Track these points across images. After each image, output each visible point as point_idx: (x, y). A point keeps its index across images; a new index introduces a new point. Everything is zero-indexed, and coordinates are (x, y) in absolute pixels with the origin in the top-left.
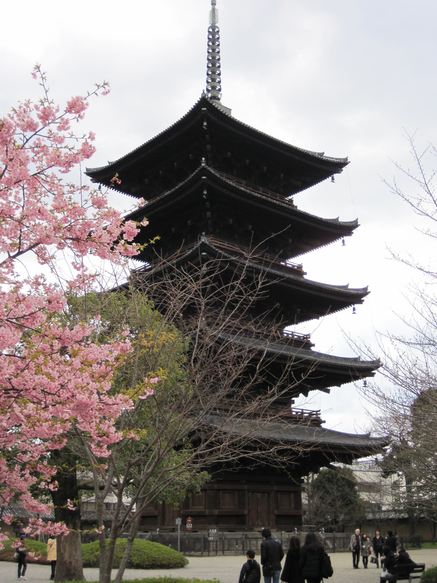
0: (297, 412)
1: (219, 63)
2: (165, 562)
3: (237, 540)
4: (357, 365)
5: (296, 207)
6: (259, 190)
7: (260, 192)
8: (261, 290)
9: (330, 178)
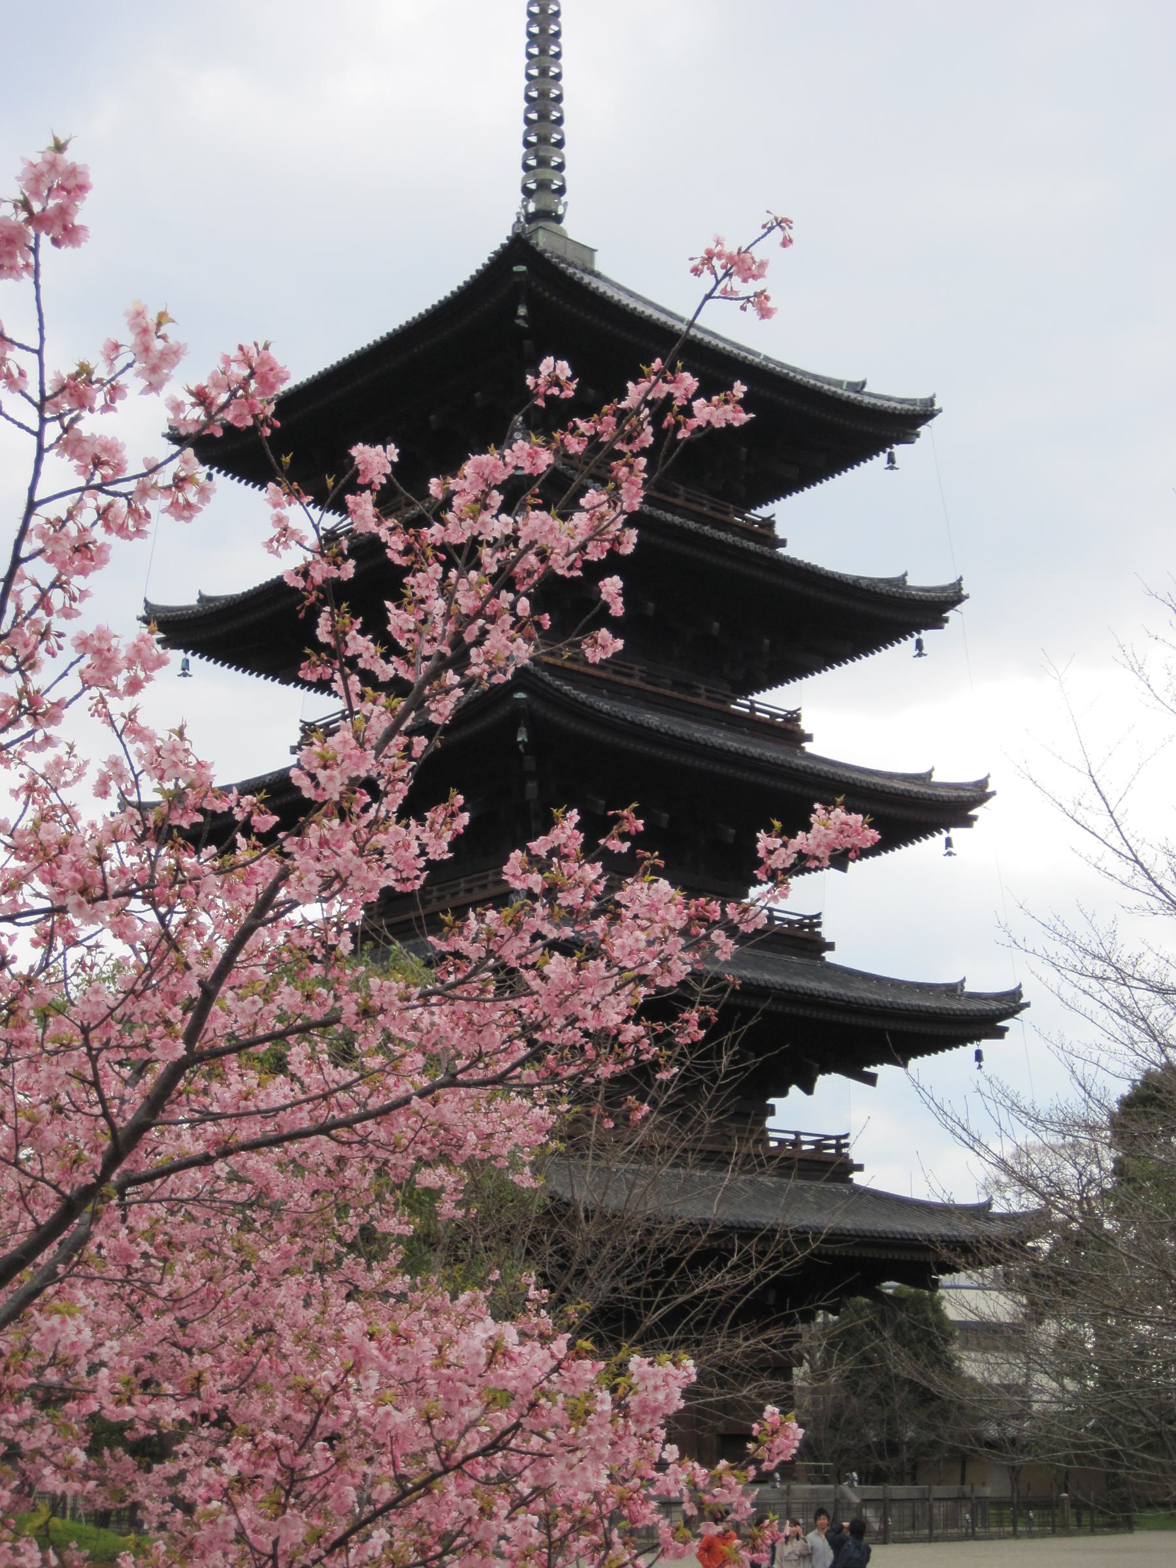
4: (955, 1005)
5: (783, 543)
6: (676, 496)
7: (679, 501)
9: (883, 457)
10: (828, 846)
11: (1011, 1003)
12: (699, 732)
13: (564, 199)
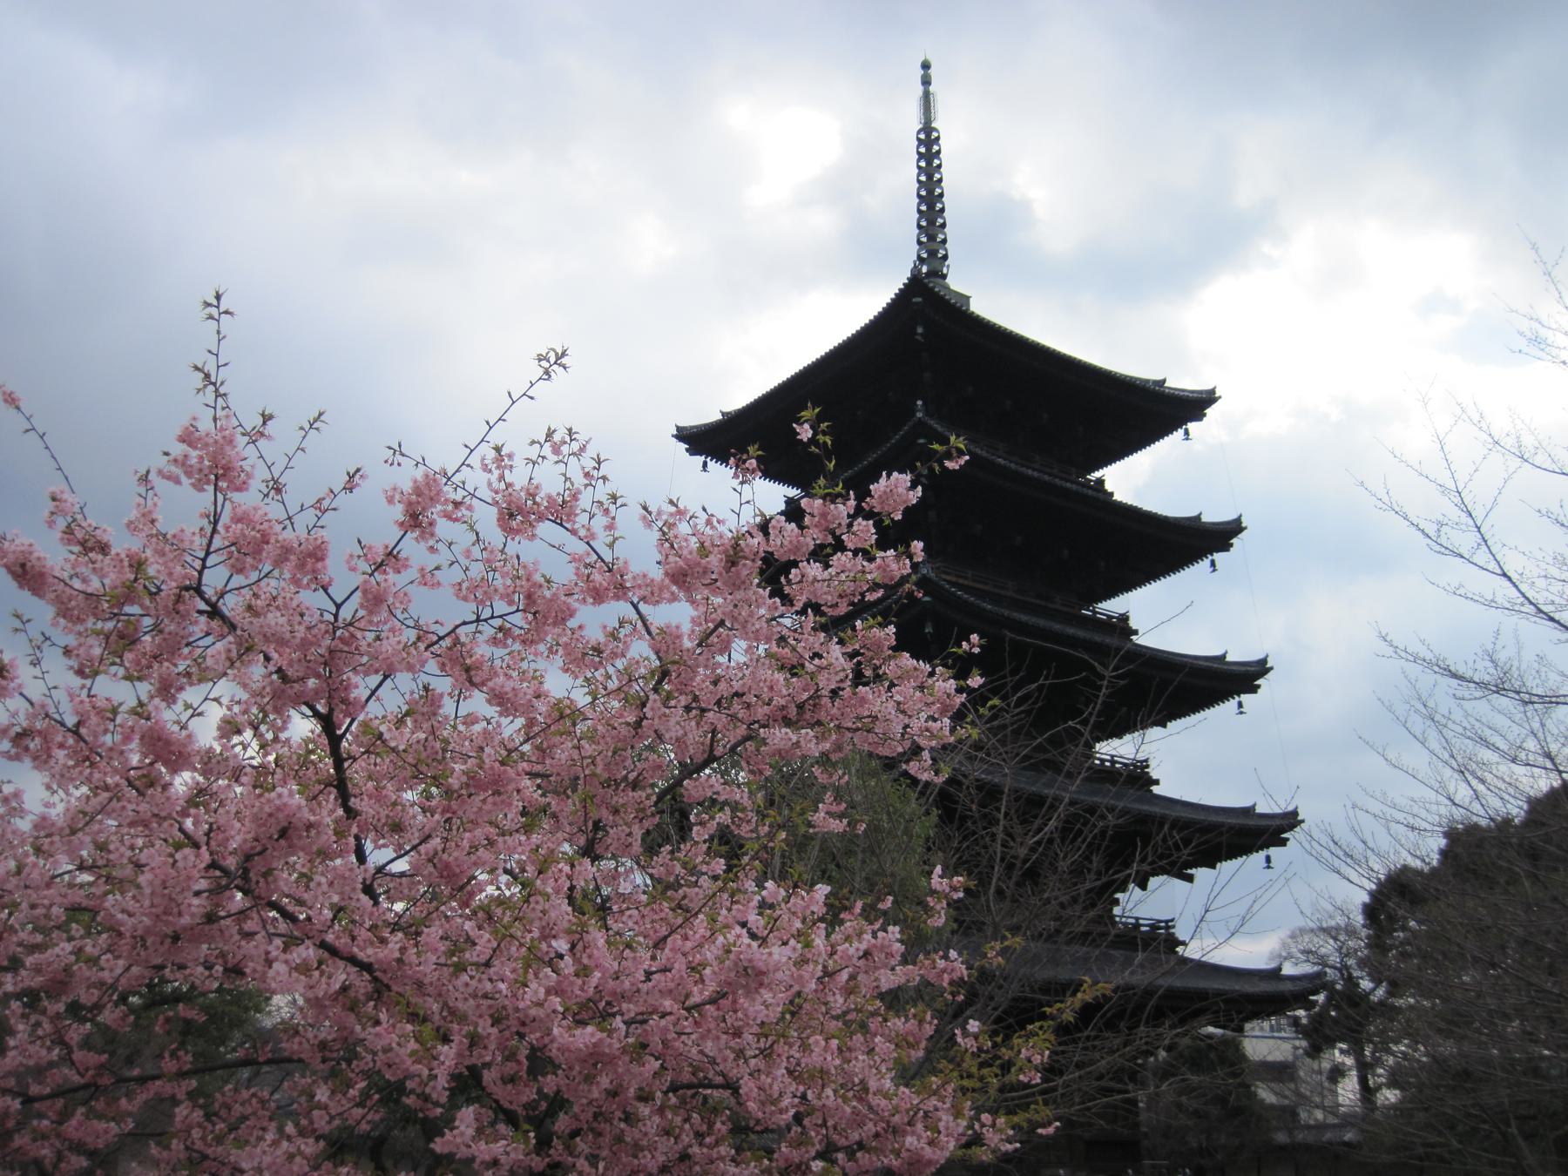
0: (1125, 924)
4: (1251, 823)
9: (1181, 432)
11: (1290, 820)
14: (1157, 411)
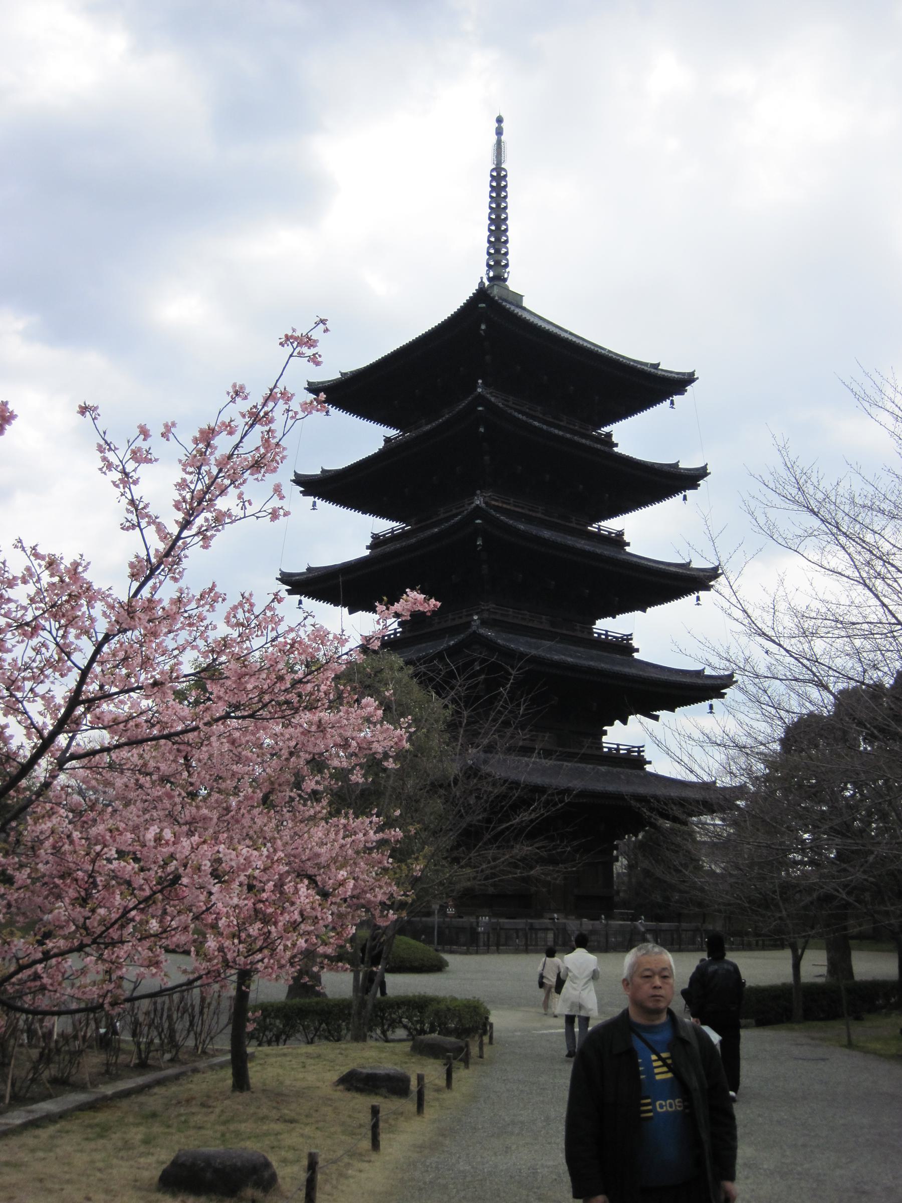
0: (610, 749)
1: (507, 225)
2: (416, 964)
3: (517, 930)
4: (700, 681)
5: (616, 445)
6: (562, 421)
8: (523, 716)
9: (668, 401)
10: (408, 610)
11: (727, 681)
12: (570, 541)
13: (507, 270)
14: (650, 387)
